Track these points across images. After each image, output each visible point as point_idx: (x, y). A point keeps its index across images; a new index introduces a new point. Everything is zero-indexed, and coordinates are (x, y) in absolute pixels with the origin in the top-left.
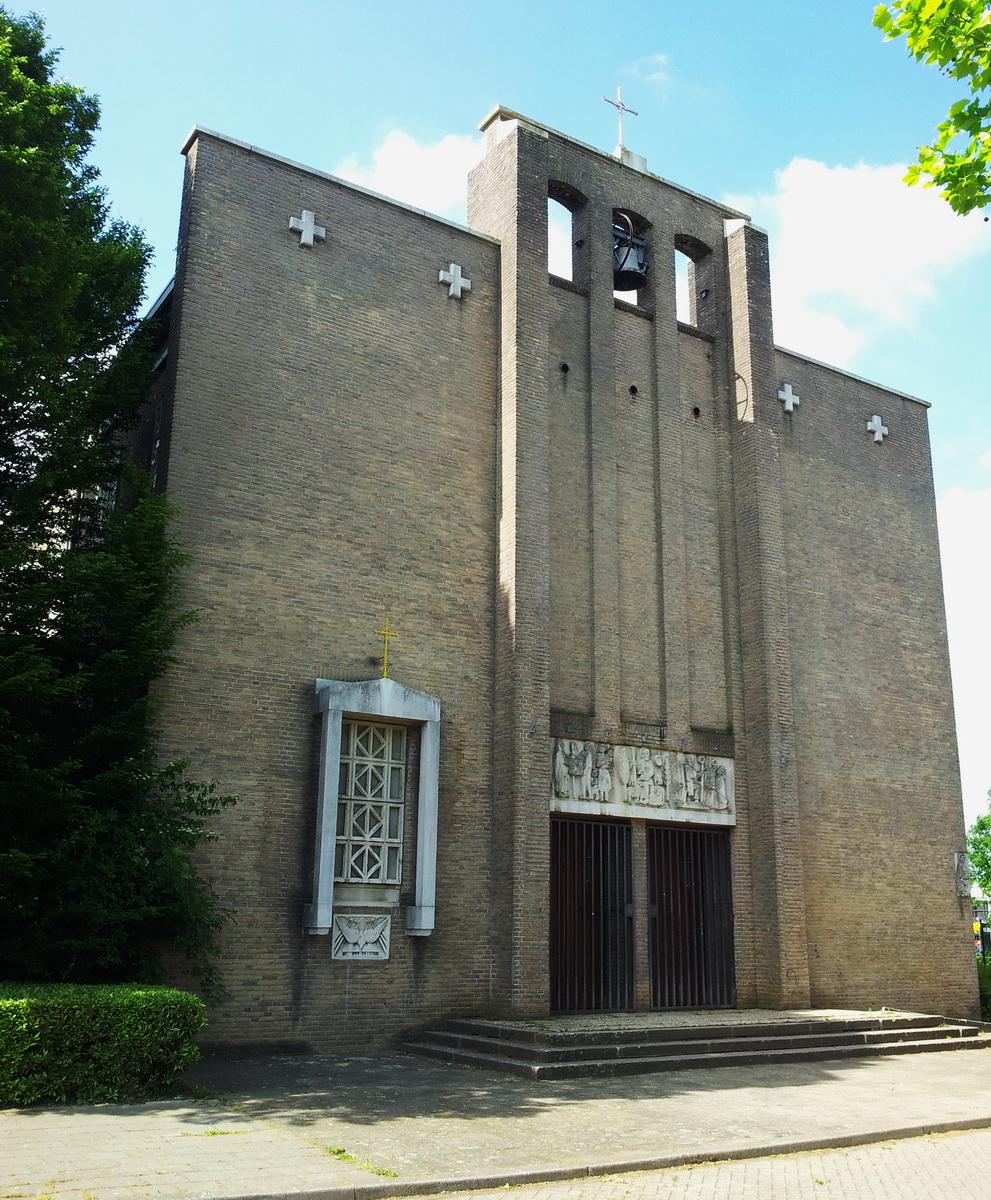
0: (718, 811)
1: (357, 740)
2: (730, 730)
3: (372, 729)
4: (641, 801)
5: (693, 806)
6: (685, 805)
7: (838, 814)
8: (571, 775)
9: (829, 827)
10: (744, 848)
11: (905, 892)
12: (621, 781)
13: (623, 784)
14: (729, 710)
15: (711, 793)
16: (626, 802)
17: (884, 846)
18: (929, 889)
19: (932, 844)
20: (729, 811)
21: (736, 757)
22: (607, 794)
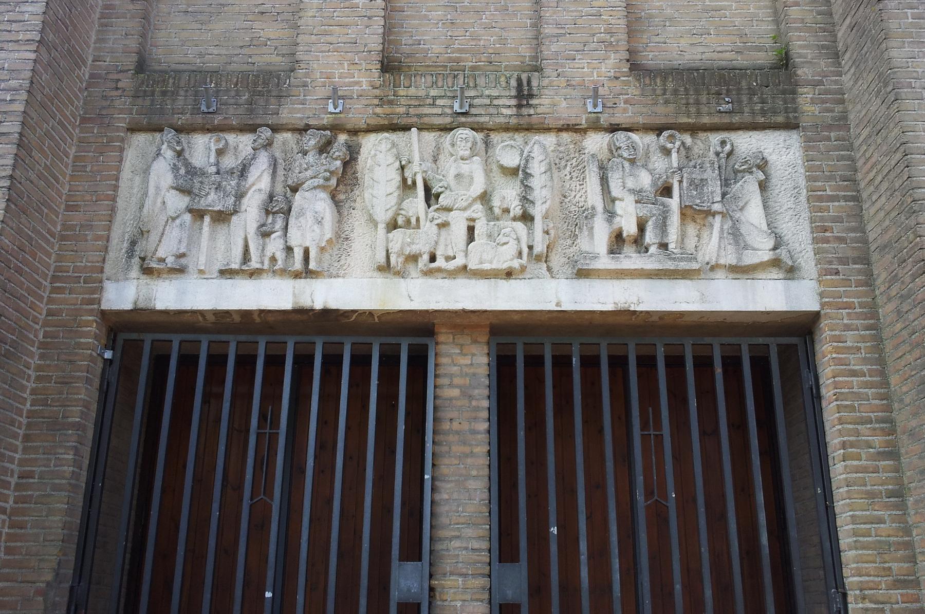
0: (739, 271)
5: (631, 260)
6: (605, 262)
10: (854, 374)
12: (373, 222)
20: (791, 272)
21: (805, 122)
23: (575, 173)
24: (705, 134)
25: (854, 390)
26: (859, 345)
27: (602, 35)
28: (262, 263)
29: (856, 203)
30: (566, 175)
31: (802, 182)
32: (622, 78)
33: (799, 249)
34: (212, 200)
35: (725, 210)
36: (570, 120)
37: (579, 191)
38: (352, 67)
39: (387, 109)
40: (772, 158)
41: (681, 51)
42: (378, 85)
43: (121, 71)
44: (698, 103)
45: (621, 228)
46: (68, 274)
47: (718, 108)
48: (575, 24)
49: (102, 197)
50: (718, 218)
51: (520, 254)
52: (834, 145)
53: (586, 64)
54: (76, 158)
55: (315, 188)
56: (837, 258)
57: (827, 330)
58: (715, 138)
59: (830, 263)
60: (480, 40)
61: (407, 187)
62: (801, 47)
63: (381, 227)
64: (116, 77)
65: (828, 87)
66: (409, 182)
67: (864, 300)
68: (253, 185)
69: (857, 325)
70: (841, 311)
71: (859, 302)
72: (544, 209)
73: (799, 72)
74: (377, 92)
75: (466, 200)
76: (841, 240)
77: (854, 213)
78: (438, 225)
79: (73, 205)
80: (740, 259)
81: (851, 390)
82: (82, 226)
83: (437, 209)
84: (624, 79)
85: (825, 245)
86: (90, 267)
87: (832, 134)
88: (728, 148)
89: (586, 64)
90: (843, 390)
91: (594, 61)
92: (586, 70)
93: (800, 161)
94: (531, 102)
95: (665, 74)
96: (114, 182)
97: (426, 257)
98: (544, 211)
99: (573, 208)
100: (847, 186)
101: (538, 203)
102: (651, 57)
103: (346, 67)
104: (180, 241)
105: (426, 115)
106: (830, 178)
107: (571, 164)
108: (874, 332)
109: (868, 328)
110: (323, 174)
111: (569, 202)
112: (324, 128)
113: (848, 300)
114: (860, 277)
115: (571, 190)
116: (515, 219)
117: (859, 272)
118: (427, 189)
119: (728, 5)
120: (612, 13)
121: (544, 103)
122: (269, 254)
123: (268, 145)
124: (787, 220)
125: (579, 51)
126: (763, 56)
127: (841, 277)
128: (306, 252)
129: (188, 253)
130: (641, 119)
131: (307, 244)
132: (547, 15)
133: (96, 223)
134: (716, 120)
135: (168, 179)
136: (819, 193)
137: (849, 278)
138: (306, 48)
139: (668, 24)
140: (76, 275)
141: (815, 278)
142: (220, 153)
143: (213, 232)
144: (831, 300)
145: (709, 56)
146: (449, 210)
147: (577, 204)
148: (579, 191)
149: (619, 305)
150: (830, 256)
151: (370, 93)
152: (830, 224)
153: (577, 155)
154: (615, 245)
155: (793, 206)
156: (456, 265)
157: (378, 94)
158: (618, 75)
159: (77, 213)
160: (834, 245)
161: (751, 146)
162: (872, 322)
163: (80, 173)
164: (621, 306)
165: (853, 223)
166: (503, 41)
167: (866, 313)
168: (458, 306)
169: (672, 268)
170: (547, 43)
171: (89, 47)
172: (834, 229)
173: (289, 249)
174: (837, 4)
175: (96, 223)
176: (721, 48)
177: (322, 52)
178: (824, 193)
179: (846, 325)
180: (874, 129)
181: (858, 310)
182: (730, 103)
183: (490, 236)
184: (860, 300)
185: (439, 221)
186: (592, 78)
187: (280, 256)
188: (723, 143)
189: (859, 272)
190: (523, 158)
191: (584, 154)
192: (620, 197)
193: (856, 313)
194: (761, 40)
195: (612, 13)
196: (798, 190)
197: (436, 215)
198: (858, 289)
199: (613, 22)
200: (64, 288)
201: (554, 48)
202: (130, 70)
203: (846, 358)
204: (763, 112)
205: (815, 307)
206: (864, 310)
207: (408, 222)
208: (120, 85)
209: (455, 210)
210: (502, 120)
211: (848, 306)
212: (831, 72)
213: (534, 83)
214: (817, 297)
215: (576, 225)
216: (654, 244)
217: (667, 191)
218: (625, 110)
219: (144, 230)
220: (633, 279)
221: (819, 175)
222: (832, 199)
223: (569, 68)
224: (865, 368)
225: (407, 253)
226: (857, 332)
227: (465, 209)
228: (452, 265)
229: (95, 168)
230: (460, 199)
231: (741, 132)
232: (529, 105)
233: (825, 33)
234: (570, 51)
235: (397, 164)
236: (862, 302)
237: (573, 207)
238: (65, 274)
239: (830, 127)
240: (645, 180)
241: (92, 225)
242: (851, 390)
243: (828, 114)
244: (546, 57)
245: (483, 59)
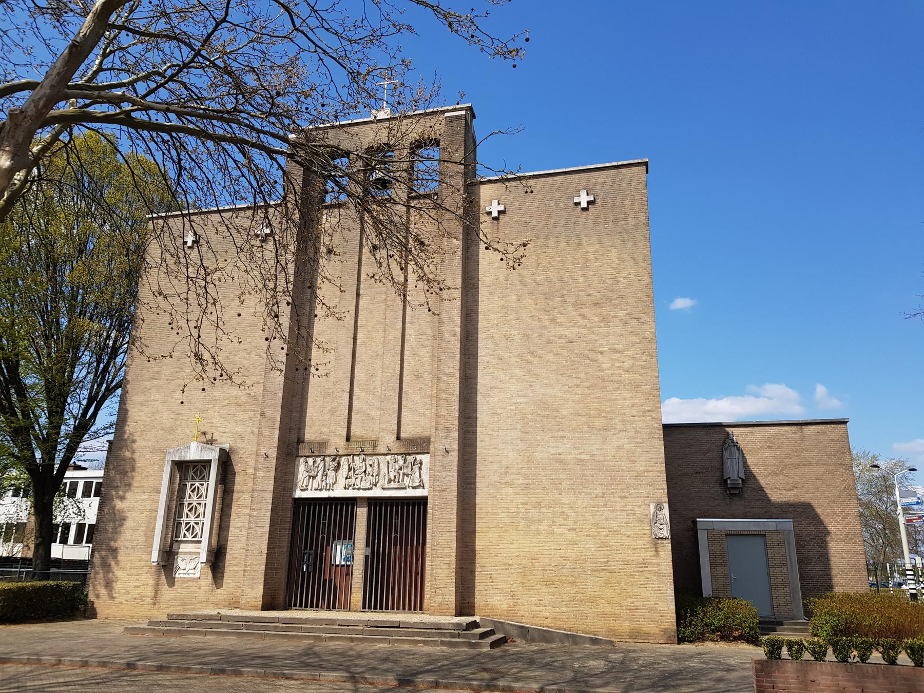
1: (192, 473)
3: (199, 466)
4: (356, 486)
7: (520, 482)
9: (510, 491)
11: (587, 535)
16: (345, 488)
17: (567, 502)
18: (616, 532)
19: (621, 497)
34: (312, 474)
61: (350, 469)
118: (354, 469)
135: (304, 469)
173: (327, 484)
204: (423, 450)
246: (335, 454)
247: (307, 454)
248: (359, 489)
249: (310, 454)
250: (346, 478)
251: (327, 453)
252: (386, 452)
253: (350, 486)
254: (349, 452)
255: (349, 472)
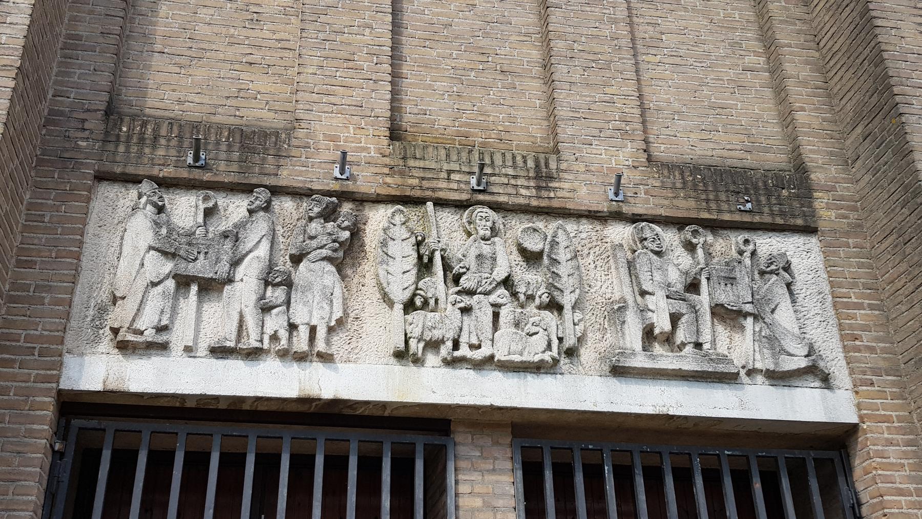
0: (778, 378)
2: (801, 169)
4: (464, 351)
5: (667, 360)
6: (640, 361)
8: (183, 282)
10: (901, 492)
13: (390, 303)
14: (787, 118)
15: (742, 328)
16: (401, 355)
20: (826, 381)
21: (822, 225)
22: (321, 333)
23: (599, 262)
24: (726, 232)
25: (903, 510)
26: (902, 461)
27: (617, 122)
28: (261, 341)
29: (882, 313)
30: (589, 264)
31: (827, 289)
32: (640, 168)
33: (831, 357)
34: (201, 267)
35: (756, 312)
36: (591, 207)
37: (605, 282)
38: (358, 131)
39: (398, 179)
40: (795, 262)
41: (692, 146)
42: (387, 153)
43: (88, 110)
44: (717, 200)
45: (653, 324)
46: (18, 344)
47: (738, 207)
48: (589, 109)
49: (64, 254)
50: (750, 320)
51: (549, 347)
52: (854, 252)
53: (603, 151)
54: (31, 206)
55: (323, 259)
56: (870, 368)
57: (869, 444)
58: (737, 238)
59: (864, 373)
60: (489, 116)
61: (424, 266)
62: (811, 151)
63: (399, 307)
64: (82, 116)
65: (841, 193)
66: (426, 260)
67: (901, 414)
68: (250, 251)
69: (898, 441)
70: (881, 424)
71: (896, 416)
72: (574, 298)
73: (812, 176)
74: (387, 160)
75: (490, 284)
76: (872, 350)
77: (881, 322)
78: (460, 309)
79: (26, 260)
80: (776, 364)
81: (901, 511)
82: (37, 286)
83: (459, 291)
84: (643, 169)
85: (856, 354)
86: (47, 336)
87: (850, 241)
88: (751, 247)
89: (603, 151)
90: (893, 510)
91: (611, 148)
92: (603, 156)
93: (821, 266)
94: (551, 185)
95: (669, 167)
96: (79, 237)
97: (449, 344)
98: (573, 300)
99: (599, 300)
100: (870, 293)
101: (567, 292)
102: (661, 150)
103: (352, 131)
104: (162, 312)
105: (441, 189)
106: (853, 286)
107: (595, 253)
108: (916, 448)
109: (908, 444)
110: (331, 245)
111: (595, 292)
112: (329, 194)
113: (885, 413)
114: (894, 390)
115: (597, 280)
116: (540, 308)
117: (894, 384)
118: (447, 267)
119: (734, 104)
120: (625, 101)
121: (564, 187)
122: (269, 331)
123: (267, 208)
124: (816, 326)
125: (595, 137)
126: (772, 157)
127: (877, 388)
128: (313, 330)
129: (170, 326)
130: (663, 212)
131: (314, 322)
132: (561, 97)
133: (55, 284)
134: (737, 217)
136: (845, 300)
137: (884, 389)
138: (308, 107)
139: (676, 118)
140: (29, 345)
141: (850, 388)
142: (209, 213)
143: (200, 301)
144: (869, 412)
145: (719, 153)
146: (471, 293)
147: (604, 295)
148: (605, 282)
149: (658, 408)
150: (863, 365)
151: (379, 161)
152: (860, 333)
153: (599, 243)
154: (647, 342)
155: (820, 312)
156: (483, 355)
157: (388, 163)
158: (636, 164)
159: (31, 270)
160: (866, 355)
161: (772, 247)
162: (911, 437)
163: (35, 224)
164: (664, 411)
165: (881, 333)
166: (512, 119)
167: (905, 428)
168: (486, 402)
169: (710, 370)
170: (562, 126)
171: (50, 79)
172: (864, 338)
173: (292, 327)
174: (843, 113)
175: (55, 284)
176: (731, 145)
177: (324, 112)
178: (849, 300)
179: (887, 440)
180: (901, 239)
181: (896, 424)
182: (749, 202)
183: (517, 325)
184: (897, 413)
185: (462, 305)
186: (611, 166)
187: (283, 334)
188: (746, 242)
189: (894, 384)
190: (547, 242)
191: (607, 243)
192: (650, 291)
193: (895, 427)
194: (768, 141)
195: (625, 101)
196: (823, 295)
197: (459, 298)
198: (894, 401)
199: (627, 110)
200: (14, 361)
201: (570, 131)
202: (100, 110)
203: (891, 475)
204: (782, 214)
205: (854, 419)
206: (903, 424)
207: (426, 303)
208: (87, 125)
209: (479, 293)
210: (522, 201)
211: (887, 419)
212: (843, 178)
213: (553, 165)
214: (854, 409)
215: (605, 318)
216: (690, 343)
217: (693, 287)
218: (647, 201)
219: (118, 294)
220: (669, 380)
221: (842, 281)
222: (859, 306)
223: (587, 153)
224: (912, 487)
225: (428, 339)
226: (898, 448)
227: (487, 293)
228: (478, 355)
229: (55, 219)
230: (484, 281)
231: (760, 233)
232: (548, 189)
233: (832, 140)
234: (586, 136)
235: (413, 240)
236: (899, 415)
237: (599, 298)
238: (14, 344)
239: (847, 234)
240: (674, 277)
241: (50, 286)
242: (901, 511)
243: (844, 220)
244: (563, 140)
245: (493, 136)
246: (334, 186)
247: (168, 172)
248: (481, 365)
249: (184, 174)
250: (409, 306)
251: (287, 176)
252: (604, 207)
253: (434, 345)
254: (411, 184)
255: (419, 277)
